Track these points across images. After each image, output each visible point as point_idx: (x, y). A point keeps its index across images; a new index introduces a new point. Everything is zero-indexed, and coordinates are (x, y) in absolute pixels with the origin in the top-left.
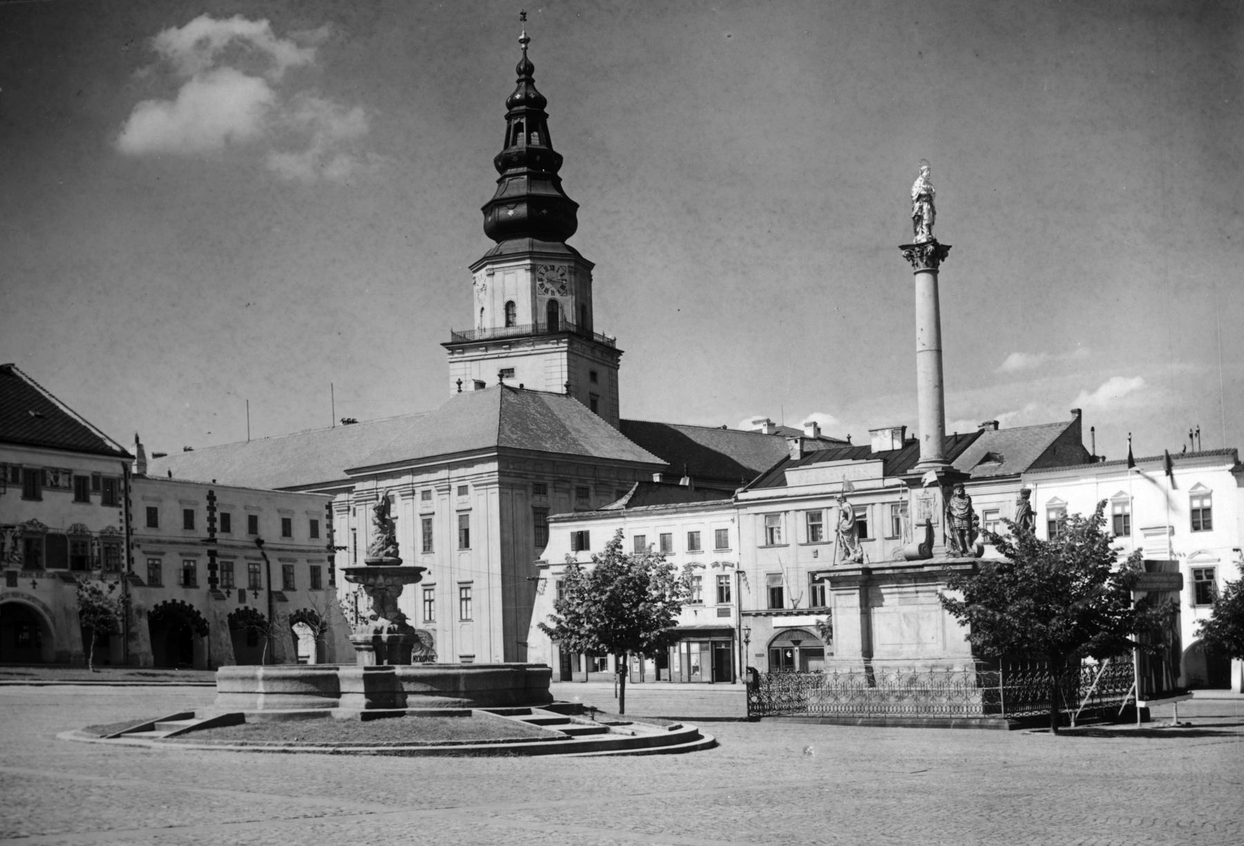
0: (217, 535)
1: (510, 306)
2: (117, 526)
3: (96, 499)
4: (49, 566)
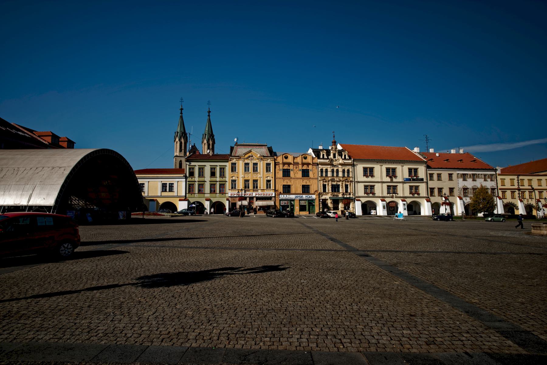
3: (489, 180)
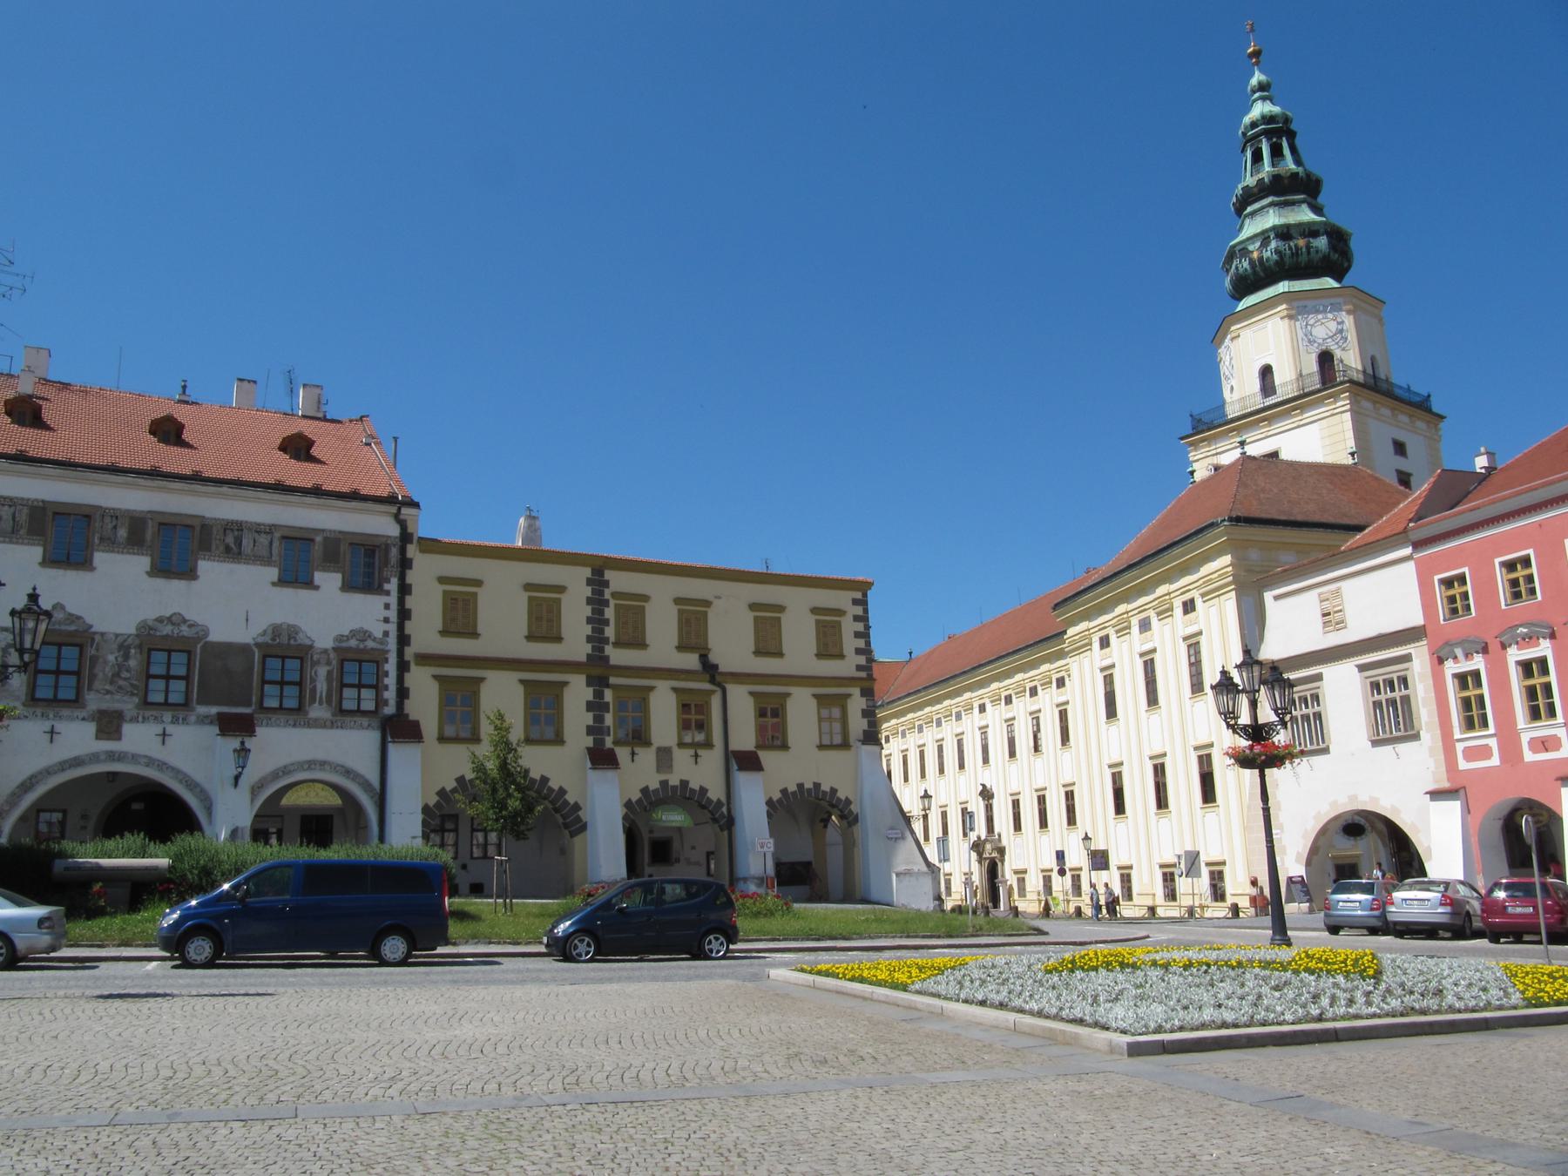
0: (609, 650)
1: (1266, 372)
2: (377, 630)
3: (330, 581)
4: (200, 702)
